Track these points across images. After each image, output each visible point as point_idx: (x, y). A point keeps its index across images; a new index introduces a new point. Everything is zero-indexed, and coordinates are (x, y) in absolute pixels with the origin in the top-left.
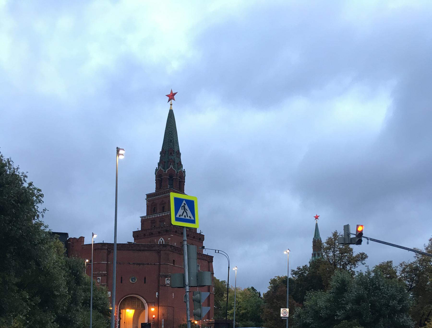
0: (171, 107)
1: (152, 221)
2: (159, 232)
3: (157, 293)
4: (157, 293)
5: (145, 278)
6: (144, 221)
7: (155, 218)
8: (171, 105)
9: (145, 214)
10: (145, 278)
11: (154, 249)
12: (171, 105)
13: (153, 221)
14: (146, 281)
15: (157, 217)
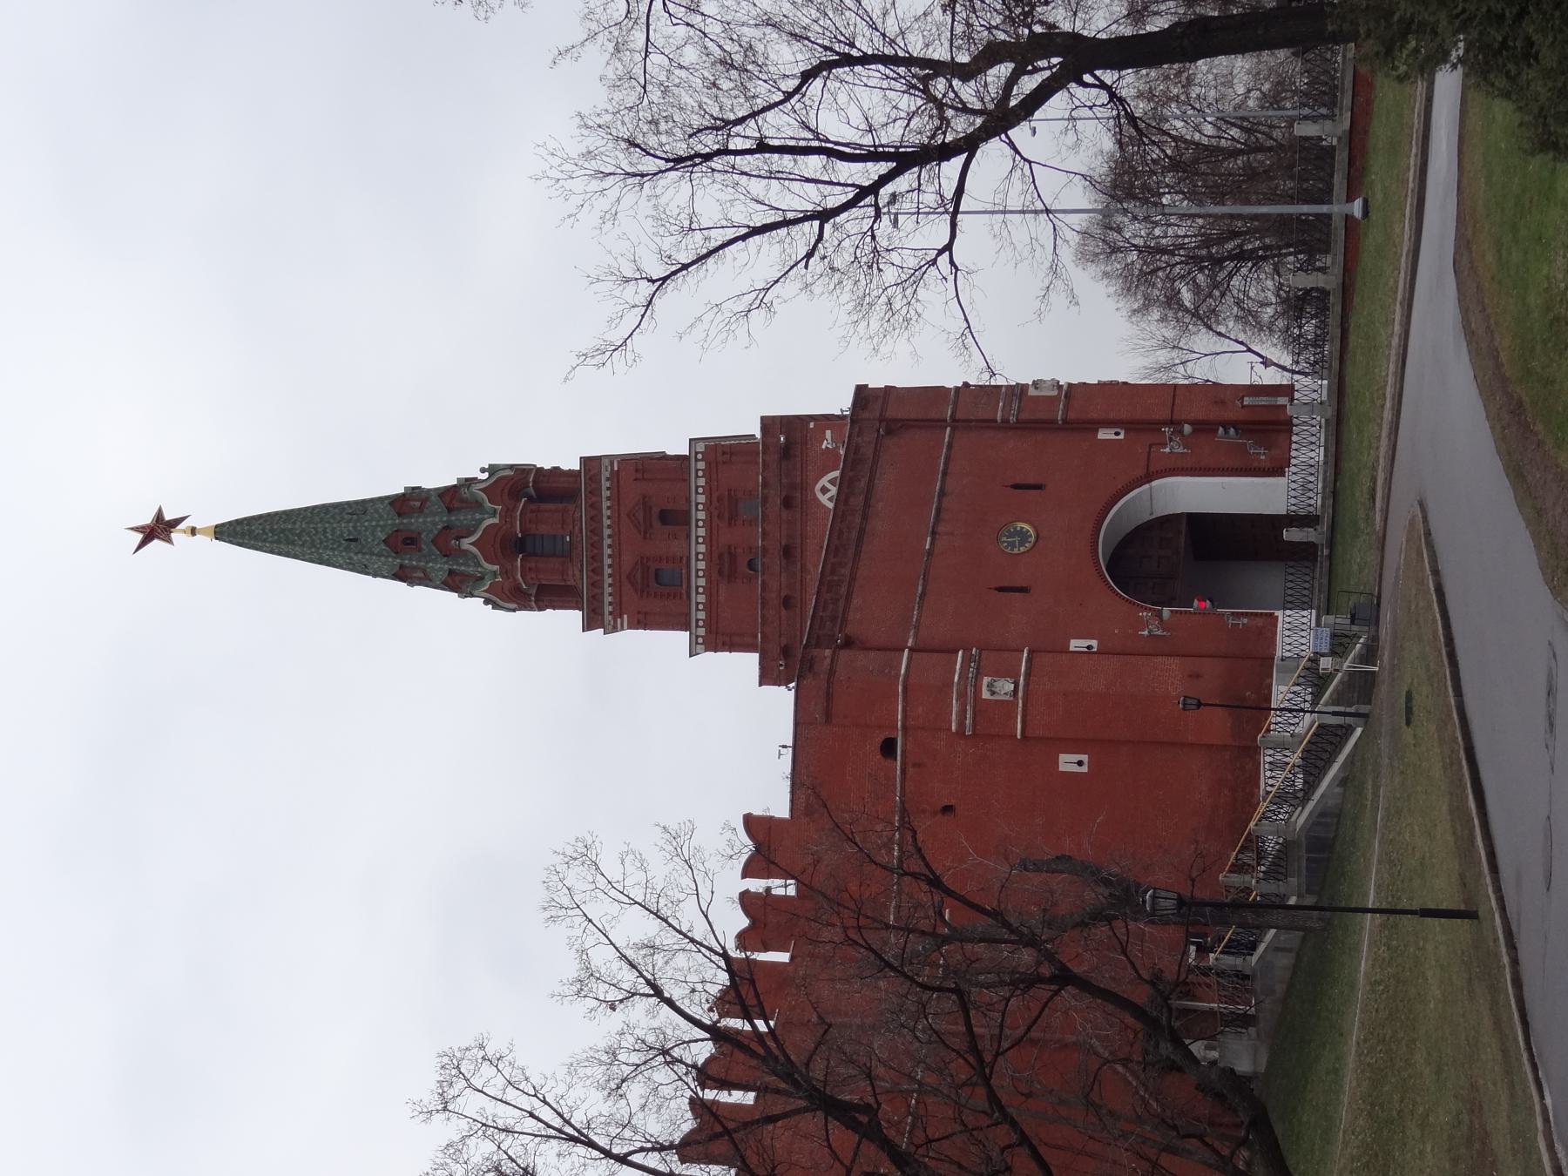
0: (204, 531)
1: (720, 573)
2: (787, 503)
3: (1105, 434)
4: (1105, 434)
5: (1016, 487)
6: (717, 638)
7: (708, 557)
8: (193, 531)
9: (681, 638)
10: (1016, 487)
11: (870, 452)
12: (193, 531)
13: (725, 565)
14: (1031, 480)
15: (710, 540)
